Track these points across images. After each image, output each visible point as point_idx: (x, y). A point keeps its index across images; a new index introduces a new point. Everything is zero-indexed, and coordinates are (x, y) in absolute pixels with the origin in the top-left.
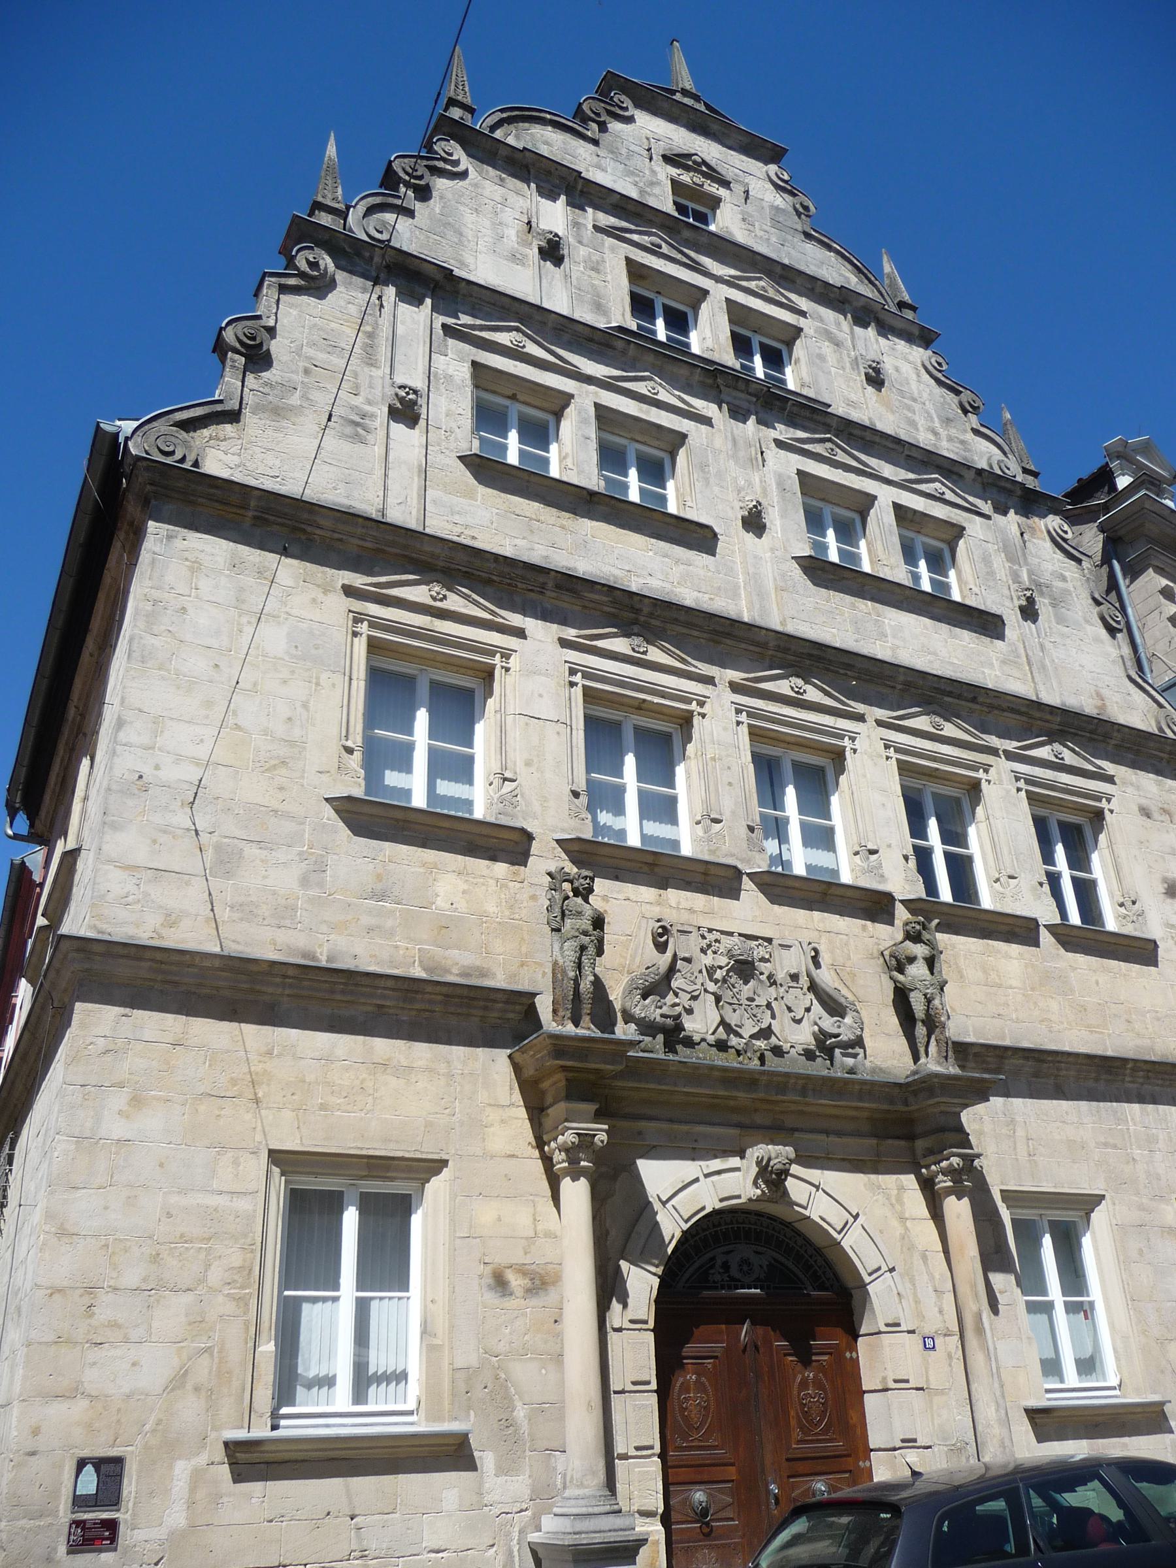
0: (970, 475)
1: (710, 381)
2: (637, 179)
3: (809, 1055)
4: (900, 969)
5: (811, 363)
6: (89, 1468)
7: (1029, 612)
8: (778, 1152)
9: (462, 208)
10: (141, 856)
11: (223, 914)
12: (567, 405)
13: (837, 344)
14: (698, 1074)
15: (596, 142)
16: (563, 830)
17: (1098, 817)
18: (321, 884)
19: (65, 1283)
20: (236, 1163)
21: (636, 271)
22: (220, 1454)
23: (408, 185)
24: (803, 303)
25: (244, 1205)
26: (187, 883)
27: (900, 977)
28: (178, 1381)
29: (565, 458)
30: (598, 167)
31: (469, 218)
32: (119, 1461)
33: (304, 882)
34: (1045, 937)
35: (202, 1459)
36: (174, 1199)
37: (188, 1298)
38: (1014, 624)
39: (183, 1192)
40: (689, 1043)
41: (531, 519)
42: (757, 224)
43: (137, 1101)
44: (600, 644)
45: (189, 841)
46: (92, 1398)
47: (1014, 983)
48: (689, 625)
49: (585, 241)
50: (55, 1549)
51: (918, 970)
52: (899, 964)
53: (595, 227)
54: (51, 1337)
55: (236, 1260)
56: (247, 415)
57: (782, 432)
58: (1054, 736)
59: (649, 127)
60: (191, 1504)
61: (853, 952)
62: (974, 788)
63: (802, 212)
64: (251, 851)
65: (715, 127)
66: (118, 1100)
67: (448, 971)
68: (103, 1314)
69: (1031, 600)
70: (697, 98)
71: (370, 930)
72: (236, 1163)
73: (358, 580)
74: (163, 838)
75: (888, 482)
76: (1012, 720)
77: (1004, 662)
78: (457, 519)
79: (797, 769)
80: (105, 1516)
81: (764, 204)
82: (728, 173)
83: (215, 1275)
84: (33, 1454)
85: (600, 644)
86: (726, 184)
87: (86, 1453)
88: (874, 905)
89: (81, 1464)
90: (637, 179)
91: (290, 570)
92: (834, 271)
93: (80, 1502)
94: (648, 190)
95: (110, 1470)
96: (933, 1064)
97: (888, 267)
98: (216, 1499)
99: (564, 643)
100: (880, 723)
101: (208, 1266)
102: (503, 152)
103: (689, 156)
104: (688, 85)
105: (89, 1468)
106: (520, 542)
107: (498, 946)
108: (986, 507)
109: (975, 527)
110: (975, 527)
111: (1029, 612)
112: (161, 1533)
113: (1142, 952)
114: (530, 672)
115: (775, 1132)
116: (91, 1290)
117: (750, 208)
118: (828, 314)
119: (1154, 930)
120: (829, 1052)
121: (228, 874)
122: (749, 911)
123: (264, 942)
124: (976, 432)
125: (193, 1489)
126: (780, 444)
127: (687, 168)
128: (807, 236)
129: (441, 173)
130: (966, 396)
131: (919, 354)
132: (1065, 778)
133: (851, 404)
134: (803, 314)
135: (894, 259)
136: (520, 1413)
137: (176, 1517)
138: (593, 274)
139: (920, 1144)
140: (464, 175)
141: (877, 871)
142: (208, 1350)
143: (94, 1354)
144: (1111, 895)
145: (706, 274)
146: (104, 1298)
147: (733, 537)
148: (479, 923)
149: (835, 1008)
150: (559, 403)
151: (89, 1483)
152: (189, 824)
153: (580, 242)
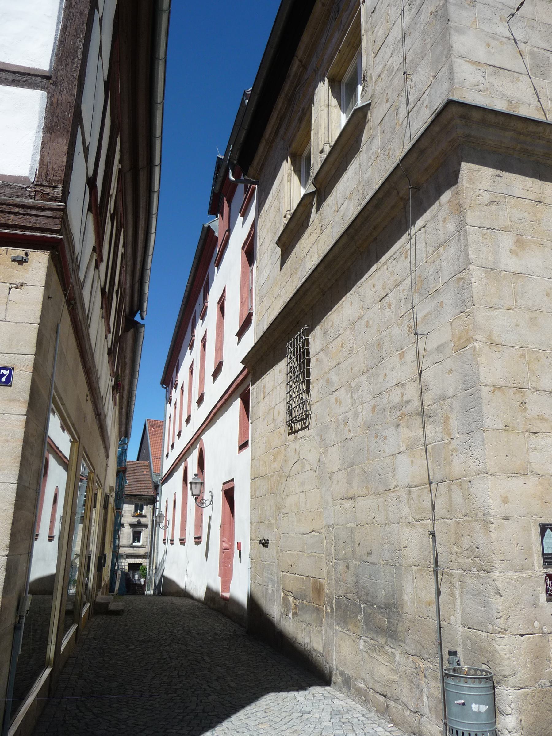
10: (481, 55)
19: (502, 383)
26: (518, 79)
43: (520, 243)
45: (510, 48)
46: (540, 476)
50: (537, 597)
66: (507, 241)
74: (493, 43)
84: (506, 518)
143: (534, 441)
146: (532, 397)
152: (509, 35)
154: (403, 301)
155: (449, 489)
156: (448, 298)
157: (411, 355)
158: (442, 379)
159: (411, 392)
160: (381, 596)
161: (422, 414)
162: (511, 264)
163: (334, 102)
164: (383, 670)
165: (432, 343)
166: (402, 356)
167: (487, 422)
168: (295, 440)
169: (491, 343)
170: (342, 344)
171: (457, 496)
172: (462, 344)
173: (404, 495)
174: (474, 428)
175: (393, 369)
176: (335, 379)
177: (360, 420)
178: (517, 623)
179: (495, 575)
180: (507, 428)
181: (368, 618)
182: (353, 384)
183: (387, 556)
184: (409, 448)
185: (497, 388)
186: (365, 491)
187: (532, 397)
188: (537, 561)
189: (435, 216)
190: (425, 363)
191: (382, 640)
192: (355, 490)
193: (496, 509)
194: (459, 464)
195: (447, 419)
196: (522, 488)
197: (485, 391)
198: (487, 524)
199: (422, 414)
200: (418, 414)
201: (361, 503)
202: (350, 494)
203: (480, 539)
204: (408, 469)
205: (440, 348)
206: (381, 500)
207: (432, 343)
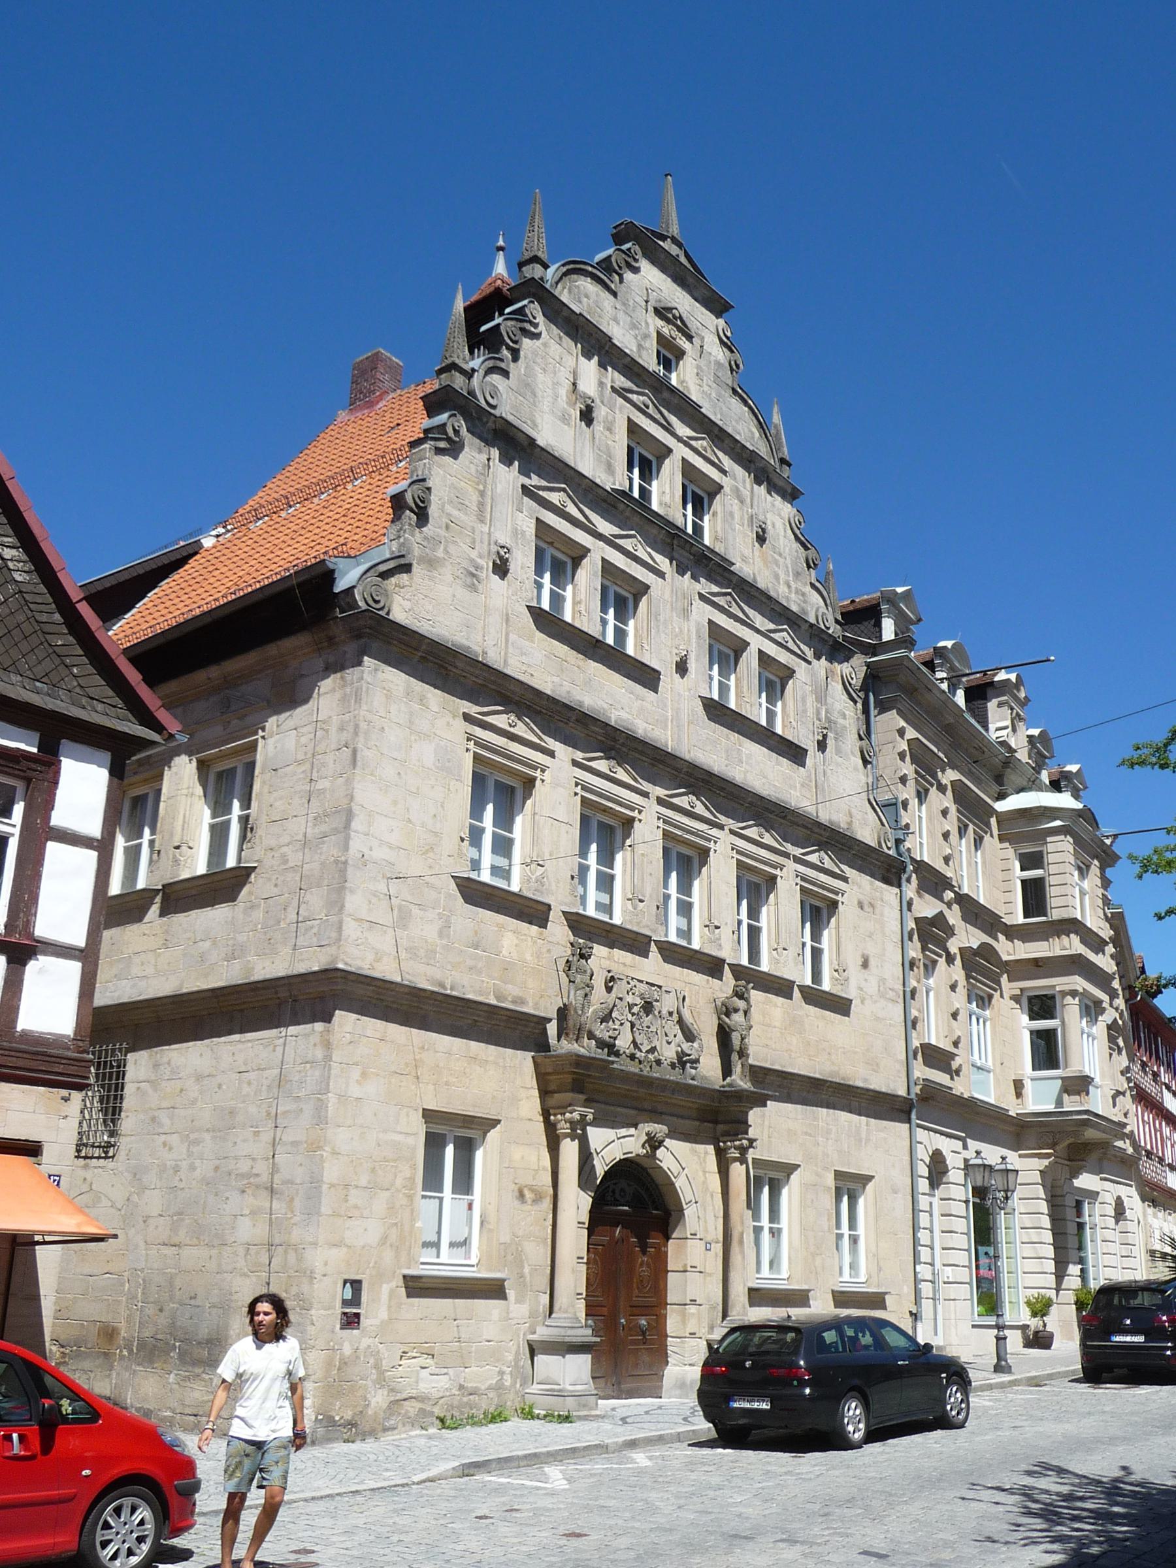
0: (805, 627)
3: (673, 1066)
4: (728, 1014)
5: (725, 521)
6: (348, 1285)
7: (822, 746)
8: (659, 1129)
9: (537, 368)
11: (403, 955)
12: (583, 557)
13: (742, 502)
14: (626, 1076)
15: (615, 294)
17: (834, 905)
18: (448, 936)
19: (335, 1182)
20: (407, 1115)
21: (633, 429)
22: (401, 1282)
23: (508, 348)
24: (727, 462)
25: (410, 1141)
27: (727, 1020)
28: (384, 1239)
29: (580, 603)
30: (616, 320)
31: (541, 377)
32: (359, 1282)
33: (441, 934)
34: (796, 993)
35: (394, 1284)
37: (387, 1194)
38: (813, 757)
39: (385, 1131)
40: (617, 1054)
43: (364, 1074)
44: (592, 764)
45: (385, 903)
47: (777, 1024)
48: (642, 753)
51: (738, 1018)
52: (728, 1011)
53: (612, 387)
54: (330, 1212)
56: (416, 568)
57: (706, 587)
58: (823, 846)
59: (649, 279)
60: (389, 1307)
61: (700, 995)
62: (772, 880)
63: (734, 368)
64: (415, 911)
65: (690, 280)
66: (356, 1073)
68: (352, 1200)
69: (825, 736)
70: (680, 245)
72: (407, 1115)
73: (474, 709)
74: (374, 900)
75: (758, 631)
76: (802, 832)
77: (802, 786)
78: (524, 659)
79: (685, 859)
80: (355, 1311)
81: (712, 358)
83: (399, 1182)
85: (592, 764)
86: (690, 338)
87: (347, 1277)
88: (712, 966)
89: (345, 1282)
91: (435, 696)
92: (744, 429)
93: (345, 1303)
95: (356, 1285)
96: (740, 1080)
97: (776, 418)
98: (399, 1305)
99: (575, 763)
100: (732, 832)
102: (565, 313)
103: (670, 309)
104: (675, 230)
105: (348, 1285)
106: (556, 679)
107: (531, 984)
108: (809, 653)
109: (801, 668)
110: (801, 668)
111: (822, 746)
112: (377, 1322)
113: (839, 1005)
114: (556, 785)
115: (655, 1115)
117: (702, 363)
118: (739, 471)
119: (851, 993)
120: (683, 1064)
121: (405, 927)
122: (652, 967)
123: (423, 976)
124: (813, 586)
125: (390, 1300)
126: (702, 597)
127: (668, 321)
128: (734, 391)
129: (524, 331)
130: (812, 553)
131: (787, 510)
132: (823, 878)
133: (744, 559)
134: (724, 472)
135: (782, 412)
136: (527, 1270)
137: (383, 1314)
139: (721, 1127)
140: (537, 336)
141: (717, 942)
142: (396, 1224)
144: (831, 963)
145: (673, 434)
146: (353, 1192)
147: (669, 679)
148: (520, 967)
149: (689, 1036)
150: (578, 555)
151: (348, 1295)
152: (386, 891)
153: (602, 402)
154: (264, 1088)
155: (286, 1252)
156: (308, 1108)
157: (267, 1137)
158: (290, 1165)
159: (262, 1168)
160: (203, 1333)
161: (272, 1191)
162: (355, 1091)
163: (199, 790)
164: (197, 1394)
165: (288, 1137)
166: (257, 1134)
167: (323, 1210)
168: (86, 1167)
169: (335, 1153)
170: (182, 1090)
172: (314, 1147)
173: (241, 1251)
174: (312, 1212)
175: (244, 1141)
176: (166, 1121)
177: (198, 1172)
178: (321, 1343)
179: (313, 1312)
180: (336, 1214)
181: (182, 1355)
182: (192, 1136)
183: (215, 1300)
184: (253, 1213)
185: (332, 1186)
186: (195, 1241)
187: (353, 1192)
188: (338, 1303)
189: (306, 1036)
190: (279, 1149)
191: (198, 1370)
192: (182, 1236)
193: (319, 1268)
194: (296, 1235)
195: (292, 1200)
196: (336, 1255)
197: (325, 1187)
198: (312, 1278)
199: (272, 1191)
200: (266, 1188)
201: (186, 1252)
202: (176, 1240)
203: (305, 1288)
204: (248, 1230)
205: (295, 1144)
206: (214, 1252)
207: (288, 1137)
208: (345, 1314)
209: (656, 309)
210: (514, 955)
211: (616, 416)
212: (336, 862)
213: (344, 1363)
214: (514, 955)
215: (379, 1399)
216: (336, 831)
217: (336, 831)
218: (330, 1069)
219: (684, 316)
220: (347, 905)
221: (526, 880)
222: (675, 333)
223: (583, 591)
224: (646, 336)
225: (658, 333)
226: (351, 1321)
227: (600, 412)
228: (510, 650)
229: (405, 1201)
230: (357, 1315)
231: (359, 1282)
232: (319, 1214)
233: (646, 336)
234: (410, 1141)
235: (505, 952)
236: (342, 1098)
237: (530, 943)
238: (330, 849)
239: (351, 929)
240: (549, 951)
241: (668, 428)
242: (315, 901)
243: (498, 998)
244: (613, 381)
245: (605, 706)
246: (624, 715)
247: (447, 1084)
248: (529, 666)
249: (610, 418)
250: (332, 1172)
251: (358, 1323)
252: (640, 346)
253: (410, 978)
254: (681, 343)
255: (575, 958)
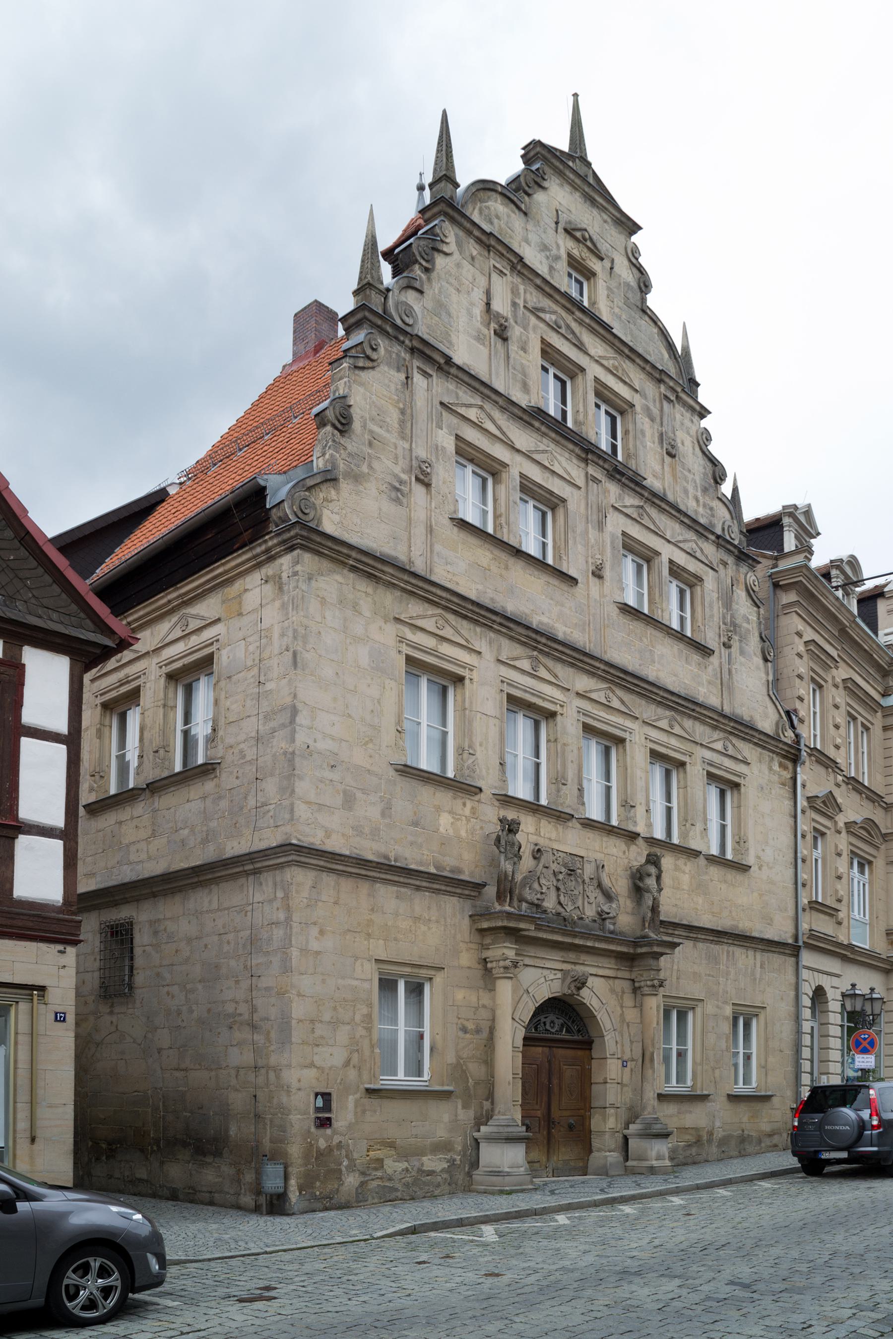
1: (584, 456)
2: (548, 254)
16: (496, 788)
20: (362, 965)
29: (500, 516)
36: (340, 981)
37: (348, 1027)
39: (343, 978)
41: (485, 569)
42: (615, 300)
46: (318, 1068)
49: (519, 322)
53: (525, 307)
55: (365, 1011)
67: (445, 869)
68: (318, 1032)
71: (412, 844)
72: (362, 965)
82: (603, 247)
83: (358, 1018)
84: (299, 1089)
90: (548, 254)
94: (554, 265)
101: (354, 1014)
106: (480, 587)
116: (312, 1021)
138: (522, 353)
143: (316, 1050)
146: (318, 1025)
153: (516, 322)
155: (267, 1072)
171: (272, 1075)
174: (285, 1039)
179: (291, 1117)
187: (318, 1025)
188: (312, 1110)
193: (295, 1084)
194: (273, 1060)
195: (268, 1033)
196: (312, 1073)
198: (288, 1092)
203: (284, 1099)
208: (318, 1118)
209: (566, 230)
210: (451, 832)
211: (530, 336)
212: (285, 753)
213: (320, 1154)
214: (451, 832)
215: (351, 1181)
216: (283, 726)
217: (283, 726)
218: (291, 928)
219: (594, 238)
220: (296, 790)
221: (458, 768)
222: (586, 254)
223: (503, 504)
224: (557, 258)
225: (569, 255)
226: (324, 1123)
227: (515, 332)
228: (436, 559)
229: (364, 1032)
230: (329, 1119)
231: (329, 1094)
232: (291, 1043)
233: (557, 258)
234: (366, 985)
235: (442, 830)
236: (304, 951)
237: (464, 822)
238: (280, 743)
239: (302, 811)
240: (482, 828)
241: (580, 347)
242: (271, 786)
243: (436, 868)
244: (525, 301)
245: (527, 611)
246: (545, 619)
247: (396, 939)
248: (454, 575)
249: (524, 338)
250: (299, 1010)
251: (330, 1125)
252: (551, 268)
253: (358, 852)
254: (591, 264)
255: (505, 833)
